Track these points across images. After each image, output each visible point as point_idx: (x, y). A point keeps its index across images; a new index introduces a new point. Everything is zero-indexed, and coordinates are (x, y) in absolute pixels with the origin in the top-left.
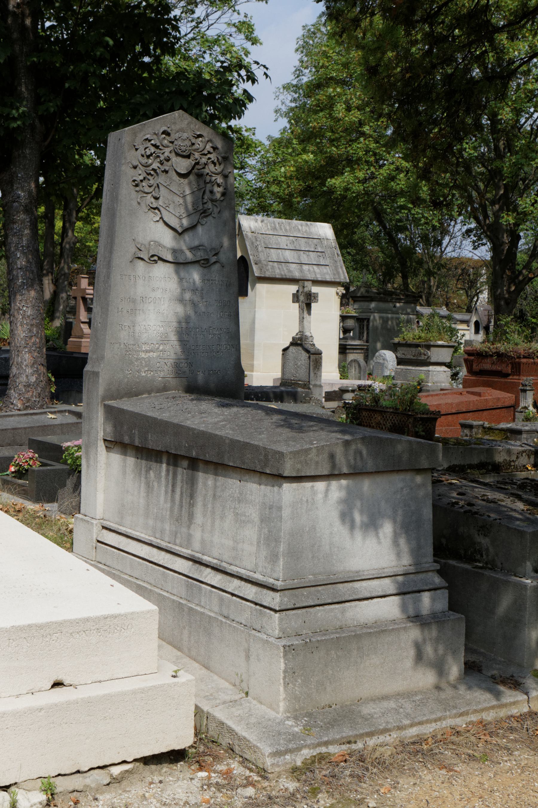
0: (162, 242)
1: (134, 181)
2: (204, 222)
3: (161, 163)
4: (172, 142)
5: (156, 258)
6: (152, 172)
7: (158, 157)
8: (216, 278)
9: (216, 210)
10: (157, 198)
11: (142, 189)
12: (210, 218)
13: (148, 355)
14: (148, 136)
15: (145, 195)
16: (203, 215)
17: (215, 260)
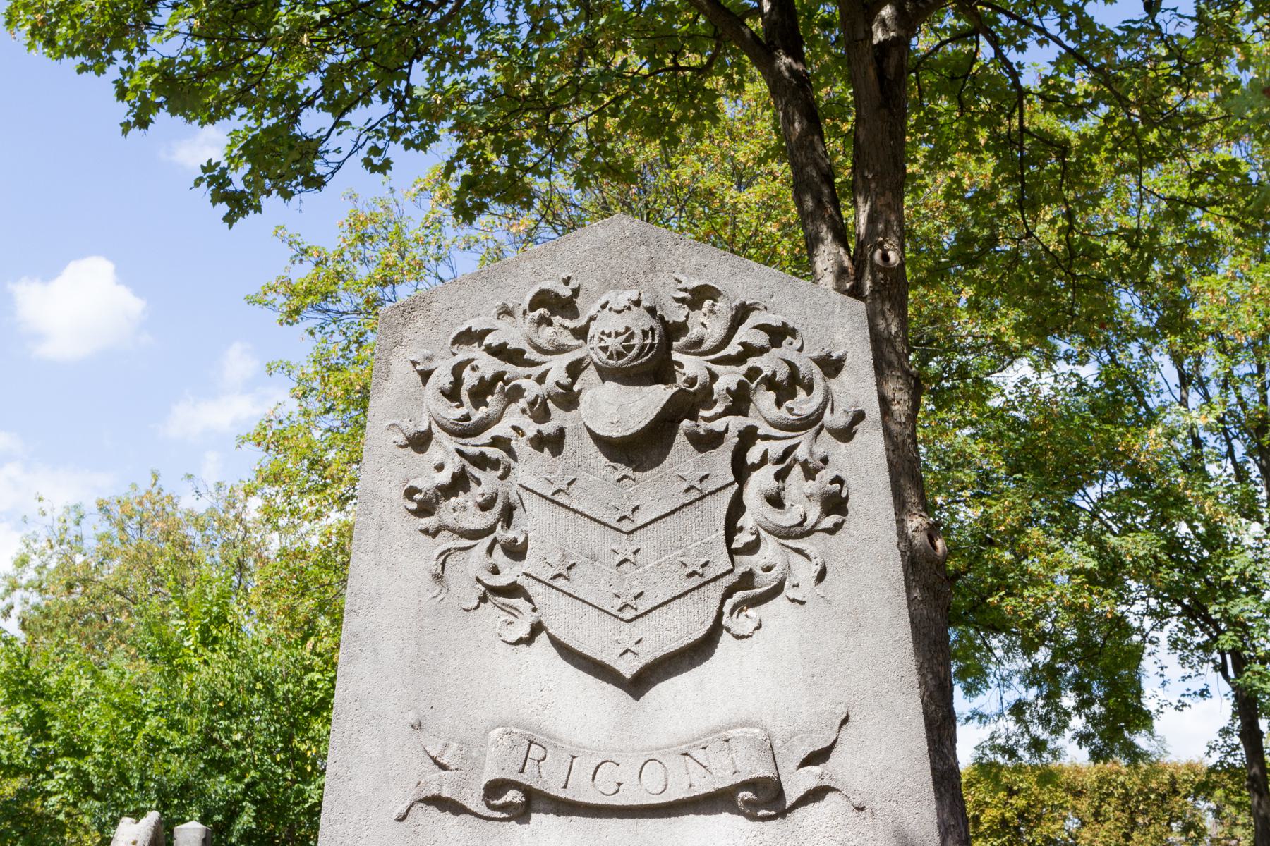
1: (410, 493)
4: (581, 333)
5: (513, 796)
6: (493, 453)
9: (804, 572)
10: (516, 552)
12: (779, 603)
14: (476, 325)
15: (466, 543)
16: (738, 596)
17: (812, 783)
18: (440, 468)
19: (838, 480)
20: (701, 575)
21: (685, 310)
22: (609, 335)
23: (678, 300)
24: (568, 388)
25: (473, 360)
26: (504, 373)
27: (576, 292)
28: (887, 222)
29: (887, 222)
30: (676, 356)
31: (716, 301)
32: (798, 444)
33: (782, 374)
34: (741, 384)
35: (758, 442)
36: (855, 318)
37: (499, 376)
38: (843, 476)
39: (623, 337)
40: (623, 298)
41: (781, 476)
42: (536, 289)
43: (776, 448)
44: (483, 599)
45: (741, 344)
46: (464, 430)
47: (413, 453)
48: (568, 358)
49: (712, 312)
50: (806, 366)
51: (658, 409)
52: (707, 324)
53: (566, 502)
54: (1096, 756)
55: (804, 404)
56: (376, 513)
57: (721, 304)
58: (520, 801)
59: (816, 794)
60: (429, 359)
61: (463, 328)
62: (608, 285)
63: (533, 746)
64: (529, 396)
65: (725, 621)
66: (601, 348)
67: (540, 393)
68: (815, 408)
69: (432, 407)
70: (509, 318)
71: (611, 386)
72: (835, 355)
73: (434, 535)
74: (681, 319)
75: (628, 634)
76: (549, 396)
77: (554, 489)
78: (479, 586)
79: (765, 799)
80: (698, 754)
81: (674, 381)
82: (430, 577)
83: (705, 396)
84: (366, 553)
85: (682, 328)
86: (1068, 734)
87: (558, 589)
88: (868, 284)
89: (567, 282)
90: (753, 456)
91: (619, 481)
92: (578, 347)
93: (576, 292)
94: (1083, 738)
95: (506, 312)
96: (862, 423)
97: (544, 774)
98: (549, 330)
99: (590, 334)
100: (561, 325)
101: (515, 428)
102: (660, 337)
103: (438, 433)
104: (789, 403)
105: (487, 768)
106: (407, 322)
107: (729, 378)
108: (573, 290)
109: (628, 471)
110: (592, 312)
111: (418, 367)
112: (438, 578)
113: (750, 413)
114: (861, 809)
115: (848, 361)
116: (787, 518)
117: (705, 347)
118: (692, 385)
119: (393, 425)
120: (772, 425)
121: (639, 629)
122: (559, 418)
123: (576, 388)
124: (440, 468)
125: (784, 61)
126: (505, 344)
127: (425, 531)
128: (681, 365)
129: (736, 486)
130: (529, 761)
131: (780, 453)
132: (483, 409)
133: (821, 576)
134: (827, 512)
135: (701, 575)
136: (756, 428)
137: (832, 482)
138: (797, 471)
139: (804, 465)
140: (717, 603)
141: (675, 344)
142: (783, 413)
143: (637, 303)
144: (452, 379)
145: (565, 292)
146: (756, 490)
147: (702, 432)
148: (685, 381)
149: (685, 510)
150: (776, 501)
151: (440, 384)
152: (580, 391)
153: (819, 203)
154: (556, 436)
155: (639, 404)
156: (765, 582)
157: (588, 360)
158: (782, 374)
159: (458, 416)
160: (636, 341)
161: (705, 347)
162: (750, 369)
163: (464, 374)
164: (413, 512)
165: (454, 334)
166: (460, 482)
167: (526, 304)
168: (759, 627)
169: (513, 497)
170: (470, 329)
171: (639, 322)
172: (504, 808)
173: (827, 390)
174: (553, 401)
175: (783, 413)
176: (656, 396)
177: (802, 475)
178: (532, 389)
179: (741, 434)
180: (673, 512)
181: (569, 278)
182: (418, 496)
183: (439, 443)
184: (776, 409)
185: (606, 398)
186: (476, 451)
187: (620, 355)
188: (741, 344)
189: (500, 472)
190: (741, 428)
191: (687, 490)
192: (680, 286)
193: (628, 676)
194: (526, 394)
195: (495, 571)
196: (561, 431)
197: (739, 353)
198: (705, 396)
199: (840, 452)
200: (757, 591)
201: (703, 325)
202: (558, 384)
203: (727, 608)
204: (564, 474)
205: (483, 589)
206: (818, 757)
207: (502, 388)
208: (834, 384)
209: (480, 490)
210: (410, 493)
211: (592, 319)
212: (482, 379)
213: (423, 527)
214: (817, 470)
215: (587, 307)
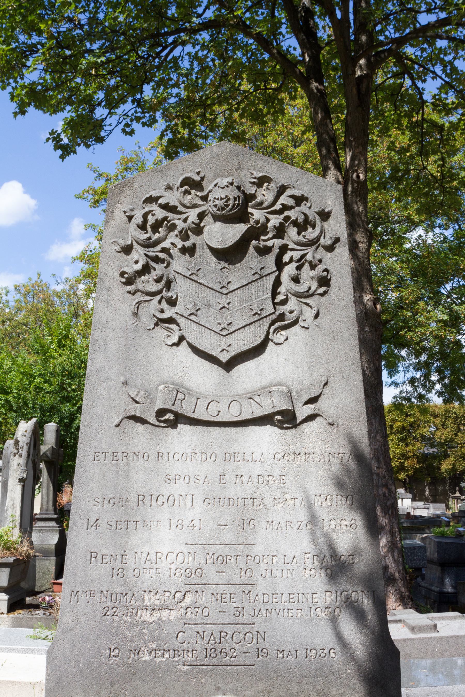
0: (187, 384)
1: (122, 274)
2: (282, 339)
3: (184, 236)
5: (169, 416)
6: (162, 255)
7: (173, 227)
8: (317, 450)
9: (309, 314)
10: (172, 302)
11: (141, 287)
12: (296, 329)
13: (157, 615)
14: (154, 194)
15: (148, 298)
16: (277, 325)
18: (136, 262)
19: (326, 270)
20: (260, 315)
21: (255, 188)
22: (218, 199)
23: (251, 183)
24: (198, 225)
25: (153, 211)
26: (167, 217)
27: (202, 179)
28: (359, 160)
29: (359, 160)
30: (250, 210)
31: (270, 183)
32: (308, 253)
33: (301, 219)
34: (281, 224)
35: (289, 252)
36: (337, 193)
37: (165, 219)
38: (329, 268)
39: (225, 200)
40: (225, 181)
41: (299, 268)
42: (183, 177)
43: (297, 255)
44: (156, 325)
45: (281, 204)
46: (148, 244)
47: (124, 255)
48: (198, 211)
49: (268, 189)
50: (312, 215)
51: (241, 235)
52: (266, 195)
53: (196, 279)
54: (446, 401)
55: (311, 234)
56: (106, 283)
57: (272, 185)
58: (172, 418)
59: (311, 418)
60: (132, 210)
61: (148, 196)
62: (218, 175)
63: (179, 394)
64: (179, 228)
65: (270, 336)
66: (214, 205)
67: (184, 227)
68: (316, 236)
69: (133, 233)
70: (170, 191)
71: (219, 224)
72: (326, 210)
73: (134, 294)
74: (253, 192)
75: (224, 342)
76: (189, 229)
77: (190, 273)
78: (155, 318)
79: (286, 419)
80: (257, 398)
81: (249, 222)
82: (131, 314)
83: (263, 230)
84: (101, 302)
85: (253, 197)
86: (434, 392)
87: (191, 320)
88: (350, 189)
89: (198, 173)
90: (286, 258)
91: (221, 269)
92: (203, 205)
93: (202, 179)
94: (440, 394)
95: (169, 188)
96: (339, 244)
97: (184, 406)
98: (189, 197)
99: (209, 199)
100: (196, 195)
101: (172, 244)
102: (242, 200)
103: (135, 245)
104: (303, 233)
105: (157, 403)
106: (122, 192)
107: (275, 221)
108: (201, 178)
109: (226, 265)
110: (210, 188)
111: (127, 214)
112: (135, 314)
113: (285, 238)
114: (332, 424)
115: (333, 213)
116: (301, 288)
117: (264, 206)
118: (257, 224)
119: (115, 242)
120: (295, 243)
121: (230, 339)
122: (193, 239)
123: (202, 225)
124: (136, 262)
125: (315, 85)
126: (168, 203)
127: (129, 292)
128: (252, 214)
129: (277, 272)
130: (177, 400)
131: (299, 257)
132: (157, 235)
133: (317, 316)
134: (320, 286)
135: (260, 315)
136: (288, 245)
137: (323, 271)
138: (307, 265)
139: (310, 263)
140: (267, 328)
141: (250, 204)
142: (301, 238)
143: (232, 184)
144: (142, 220)
145: (197, 178)
146: (287, 275)
147: (261, 247)
148: (254, 222)
149: (253, 283)
150: (296, 280)
151: (137, 222)
152: (204, 226)
153: (329, 151)
154: (191, 247)
155: (232, 233)
156: (290, 318)
157: (208, 212)
158: (301, 219)
159: (145, 238)
160: (231, 202)
161: (264, 206)
162: (285, 217)
163: (148, 218)
164: (124, 283)
165: (144, 198)
166: (146, 269)
167: (178, 184)
168: (287, 339)
169: (171, 276)
170: (151, 196)
171: (232, 193)
172: (165, 421)
173: (322, 227)
174: (191, 231)
175: (301, 238)
176: (240, 229)
177: (309, 268)
178: (180, 225)
179: (280, 248)
180: (247, 285)
181: (199, 172)
182: (126, 276)
183: (136, 251)
184: (297, 236)
185: (216, 229)
186: (154, 254)
187: (223, 209)
188: (281, 204)
189: (165, 265)
190: (280, 245)
191: (254, 274)
192: (253, 176)
193: (224, 361)
194: (178, 227)
195: (162, 311)
196: (194, 245)
197: (280, 209)
198: (263, 230)
199: (327, 257)
200: (286, 322)
201: (264, 195)
202: (193, 222)
203: (272, 330)
204: (195, 266)
205: (156, 320)
206: (313, 400)
207: (167, 224)
208: (326, 224)
209: (155, 273)
210: (122, 274)
211: (210, 191)
212: (157, 220)
213: (128, 290)
214: (316, 266)
215: (208, 186)
